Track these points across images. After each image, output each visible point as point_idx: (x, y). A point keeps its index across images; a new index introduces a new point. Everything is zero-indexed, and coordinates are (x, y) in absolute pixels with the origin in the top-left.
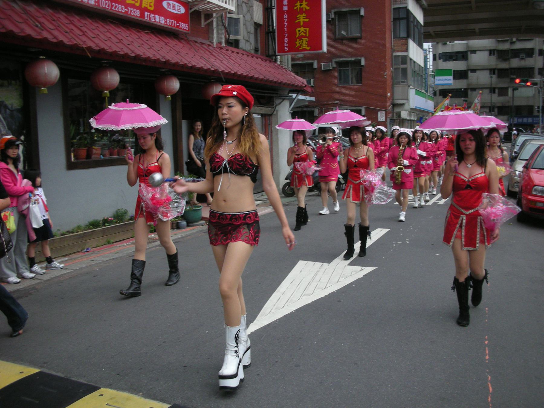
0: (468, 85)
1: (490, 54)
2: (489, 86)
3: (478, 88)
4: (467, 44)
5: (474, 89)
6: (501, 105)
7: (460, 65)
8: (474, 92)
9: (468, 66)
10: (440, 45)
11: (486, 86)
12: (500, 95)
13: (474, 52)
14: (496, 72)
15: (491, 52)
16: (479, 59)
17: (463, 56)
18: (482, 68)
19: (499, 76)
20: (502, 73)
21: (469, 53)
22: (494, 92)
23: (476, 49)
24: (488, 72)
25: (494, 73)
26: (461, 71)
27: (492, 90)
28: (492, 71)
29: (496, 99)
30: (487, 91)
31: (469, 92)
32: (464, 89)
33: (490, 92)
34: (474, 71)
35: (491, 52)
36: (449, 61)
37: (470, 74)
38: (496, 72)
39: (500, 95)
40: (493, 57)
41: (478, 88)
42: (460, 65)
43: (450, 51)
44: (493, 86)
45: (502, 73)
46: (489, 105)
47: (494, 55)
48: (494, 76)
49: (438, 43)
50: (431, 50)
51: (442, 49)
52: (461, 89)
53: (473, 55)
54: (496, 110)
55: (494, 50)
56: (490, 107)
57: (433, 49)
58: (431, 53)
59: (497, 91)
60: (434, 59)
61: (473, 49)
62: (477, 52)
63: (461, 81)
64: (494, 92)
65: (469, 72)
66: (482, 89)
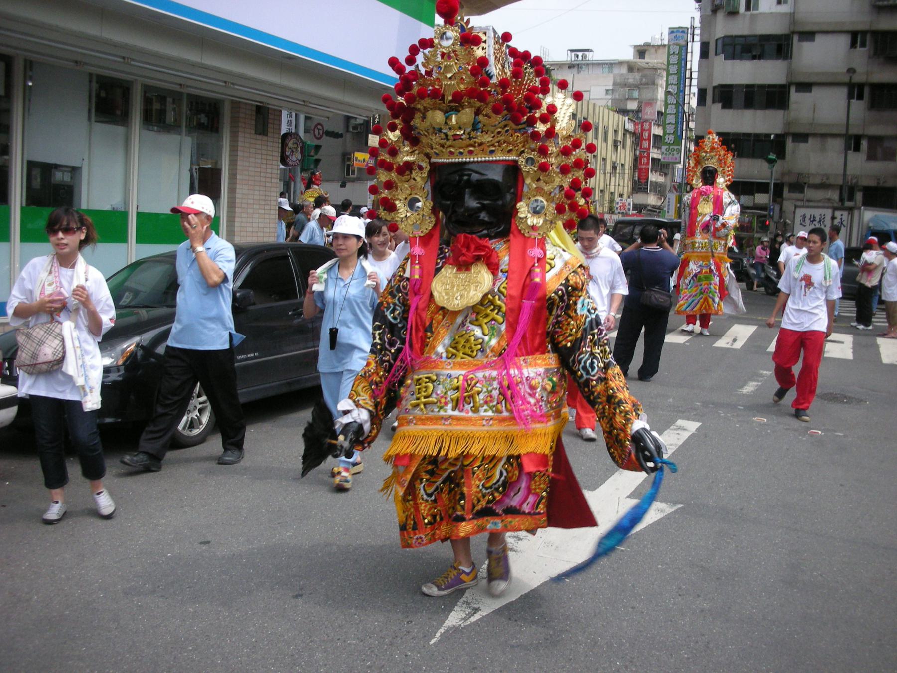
0: (788, 124)
1: (853, 45)
2: (844, 132)
3: (815, 135)
4: (792, 15)
5: (802, 137)
6: (872, 184)
7: (766, 72)
8: (802, 145)
9: (790, 73)
10: (720, 15)
11: (835, 131)
12: (871, 157)
13: (808, 35)
14: (866, 91)
15: (856, 38)
16: (822, 56)
17: (777, 46)
18: (829, 80)
19: (874, 105)
20: (881, 97)
21: (796, 38)
22: (857, 148)
23: (815, 28)
24: (843, 92)
25: (860, 97)
26: (770, 86)
27: (853, 142)
28: (855, 90)
29: (861, 167)
30: (837, 144)
31: (790, 144)
32: (777, 135)
33: (847, 148)
34: (805, 87)
35: (856, 38)
36: (741, 58)
37: (795, 96)
38: (866, 91)
39: (871, 156)
40: (861, 53)
41: (815, 135)
42: (766, 72)
43: (746, 32)
44: (853, 131)
45: (881, 97)
46: (840, 182)
47: (863, 45)
48: (859, 107)
49: (715, 10)
50: (697, 32)
51: (723, 28)
52: (769, 135)
53: (806, 45)
54: (859, 196)
55: (864, 33)
56: (841, 188)
57: (702, 28)
58: (697, 38)
59: (864, 144)
60: (704, 54)
61: (808, 28)
62: (819, 38)
63: (770, 113)
64: (857, 148)
65: (793, 89)
66: (824, 136)
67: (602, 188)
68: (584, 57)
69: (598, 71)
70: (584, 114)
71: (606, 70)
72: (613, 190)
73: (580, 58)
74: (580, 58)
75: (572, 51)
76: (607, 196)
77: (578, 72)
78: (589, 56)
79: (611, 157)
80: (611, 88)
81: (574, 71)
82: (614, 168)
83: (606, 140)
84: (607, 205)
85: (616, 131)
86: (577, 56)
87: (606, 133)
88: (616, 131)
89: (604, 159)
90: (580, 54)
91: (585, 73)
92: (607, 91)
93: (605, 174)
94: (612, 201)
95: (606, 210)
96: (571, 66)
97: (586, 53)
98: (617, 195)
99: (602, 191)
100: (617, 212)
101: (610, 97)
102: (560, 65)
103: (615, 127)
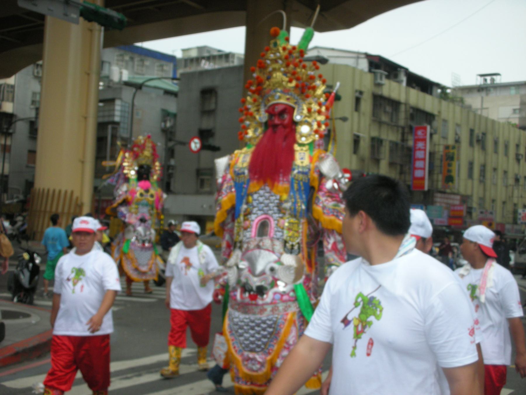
67: (504, 199)
68: (493, 80)
69: (504, 93)
70: (483, 129)
71: (513, 91)
72: (515, 200)
73: (489, 82)
74: (489, 82)
75: (482, 76)
76: (510, 207)
77: (487, 95)
78: (498, 80)
79: (513, 168)
80: (518, 107)
81: (483, 94)
82: (517, 180)
83: (506, 154)
84: (511, 216)
85: (518, 146)
86: (486, 80)
87: (506, 147)
88: (518, 146)
89: (505, 172)
90: (488, 78)
91: (493, 94)
92: (515, 110)
93: (507, 187)
94: (515, 212)
95: (511, 220)
96: (480, 89)
97: (495, 77)
98: (520, 206)
99: (504, 203)
100: (519, 222)
101: (517, 116)
102: (469, 90)
103: (516, 142)
